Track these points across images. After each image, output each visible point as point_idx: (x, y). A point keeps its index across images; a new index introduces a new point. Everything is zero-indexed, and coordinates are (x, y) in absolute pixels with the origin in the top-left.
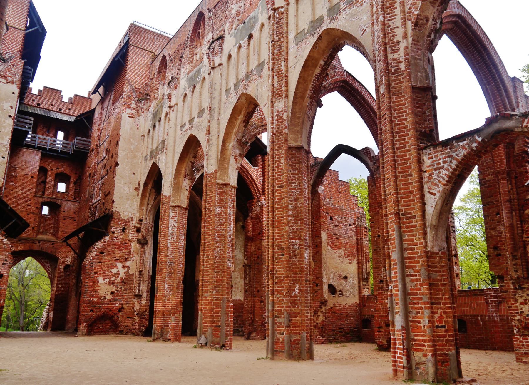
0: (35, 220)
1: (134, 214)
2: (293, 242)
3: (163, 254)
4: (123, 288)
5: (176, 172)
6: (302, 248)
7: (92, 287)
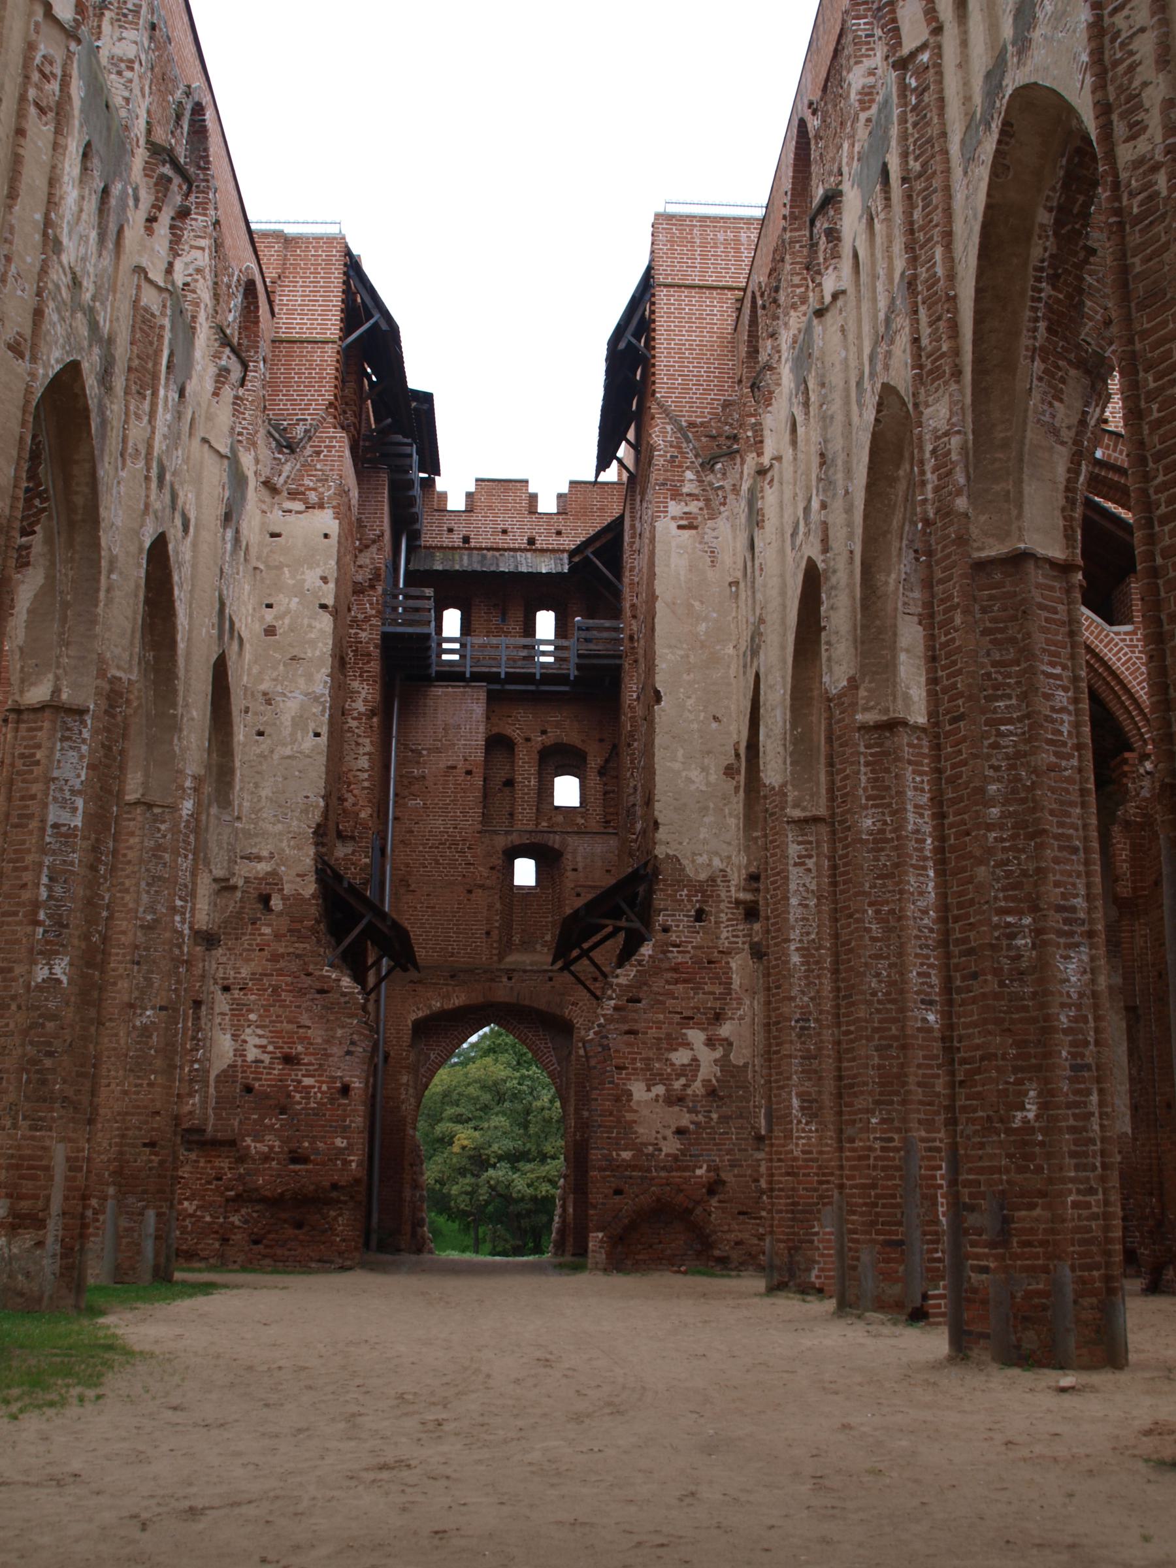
0: (490, 907)
1: (729, 857)
2: (1009, 925)
3: (778, 994)
4: (715, 1116)
5: (794, 698)
6: (1045, 943)
7: (611, 1114)
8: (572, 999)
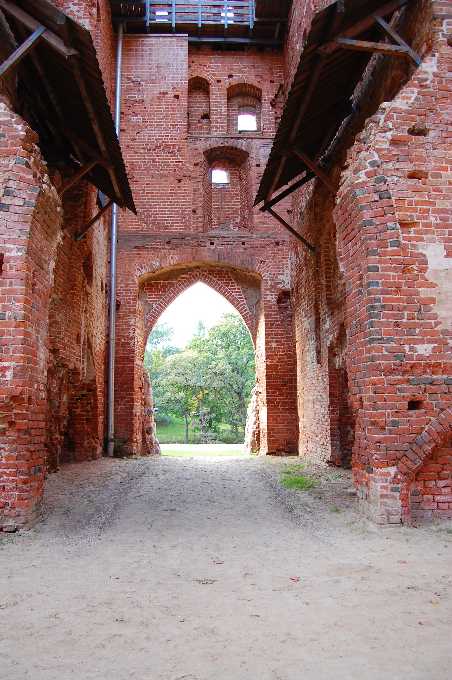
0: (195, 192)
8: (260, 258)
